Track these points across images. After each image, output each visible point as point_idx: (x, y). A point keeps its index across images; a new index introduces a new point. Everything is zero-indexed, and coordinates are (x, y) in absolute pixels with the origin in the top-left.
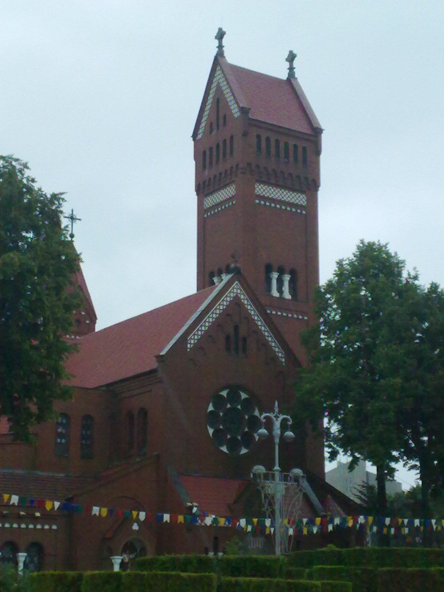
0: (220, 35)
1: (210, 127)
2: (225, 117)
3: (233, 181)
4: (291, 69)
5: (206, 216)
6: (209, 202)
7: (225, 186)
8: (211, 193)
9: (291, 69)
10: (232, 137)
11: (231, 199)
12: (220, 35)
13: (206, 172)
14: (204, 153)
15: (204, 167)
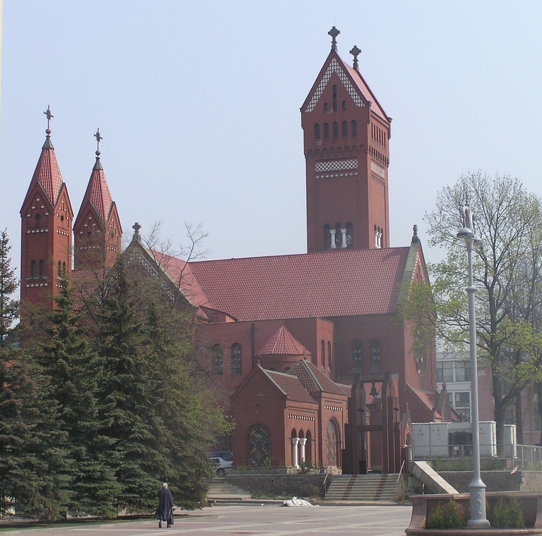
0: (334, 33)
1: (323, 105)
2: (344, 102)
3: (356, 157)
4: (356, 61)
5: (317, 177)
6: (321, 167)
7: (345, 159)
8: (327, 161)
9: (356, 61)
10: (354, 121)
11: (353, 170)
12: (334, 33)
13: (320, 143)
14: (317, 125)
15: (317, 137)
